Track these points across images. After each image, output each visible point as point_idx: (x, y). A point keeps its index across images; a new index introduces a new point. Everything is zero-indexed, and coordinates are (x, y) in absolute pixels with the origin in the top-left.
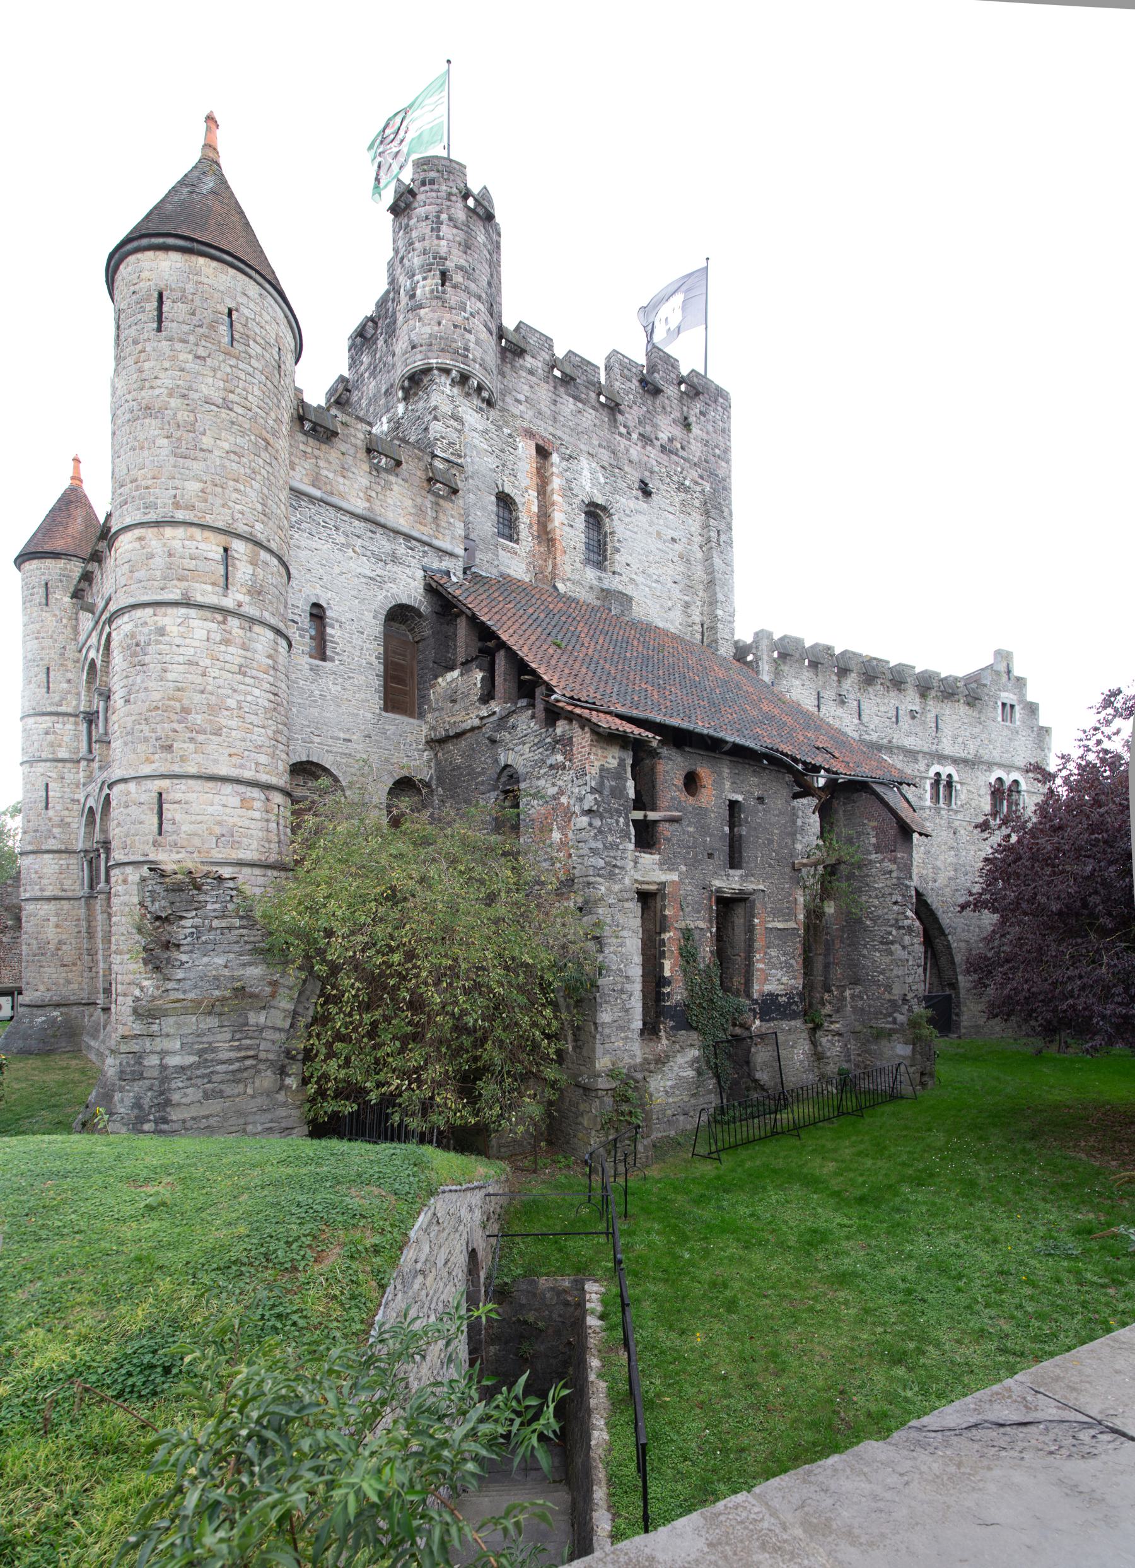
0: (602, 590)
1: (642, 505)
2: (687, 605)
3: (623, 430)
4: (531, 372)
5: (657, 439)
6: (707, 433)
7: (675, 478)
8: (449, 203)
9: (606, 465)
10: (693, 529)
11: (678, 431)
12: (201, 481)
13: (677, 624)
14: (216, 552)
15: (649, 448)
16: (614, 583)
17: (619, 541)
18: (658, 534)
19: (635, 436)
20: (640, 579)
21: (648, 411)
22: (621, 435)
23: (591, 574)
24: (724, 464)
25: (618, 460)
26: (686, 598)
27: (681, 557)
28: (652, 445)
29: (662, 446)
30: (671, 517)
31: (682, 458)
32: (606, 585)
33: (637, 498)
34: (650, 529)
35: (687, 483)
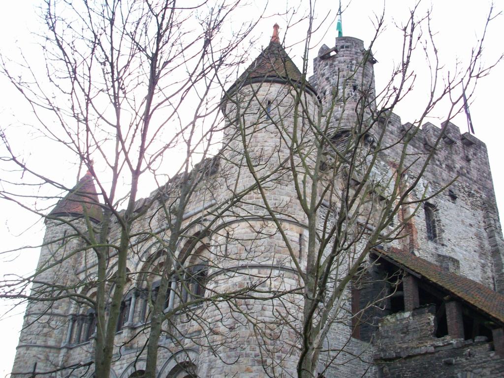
0: (439, 256)
1: (450, 204)
2: (483, 266)
3: (438, 163)
4: (392, 133)
5: (455, 168)
6: (479, 164)
7: (466, 189)
8: (356, 56)
9: (432, 181)
10: (480, 218)
11: (464, 164)
12: (290, 196)
13: (480, 277)
14: (296, 237)
15: (451, 173)
16: (444, 251)
17: (443, 226)
18: (462, 221)
19: (444, 166)
20: (457, 249)
21: (449, 154)
22: (437, 165)
23: (431, 245)
24: (489, 181)
25: (437, 179)
26: (483, 261)
27: (476, 235)
28: (453, 171)
29: (458, 171)
30: (468, 211)
31: (468, 178)
32: (440, 252)
33: (449, 201)
34: (458, 218)
35: (472, 192)
